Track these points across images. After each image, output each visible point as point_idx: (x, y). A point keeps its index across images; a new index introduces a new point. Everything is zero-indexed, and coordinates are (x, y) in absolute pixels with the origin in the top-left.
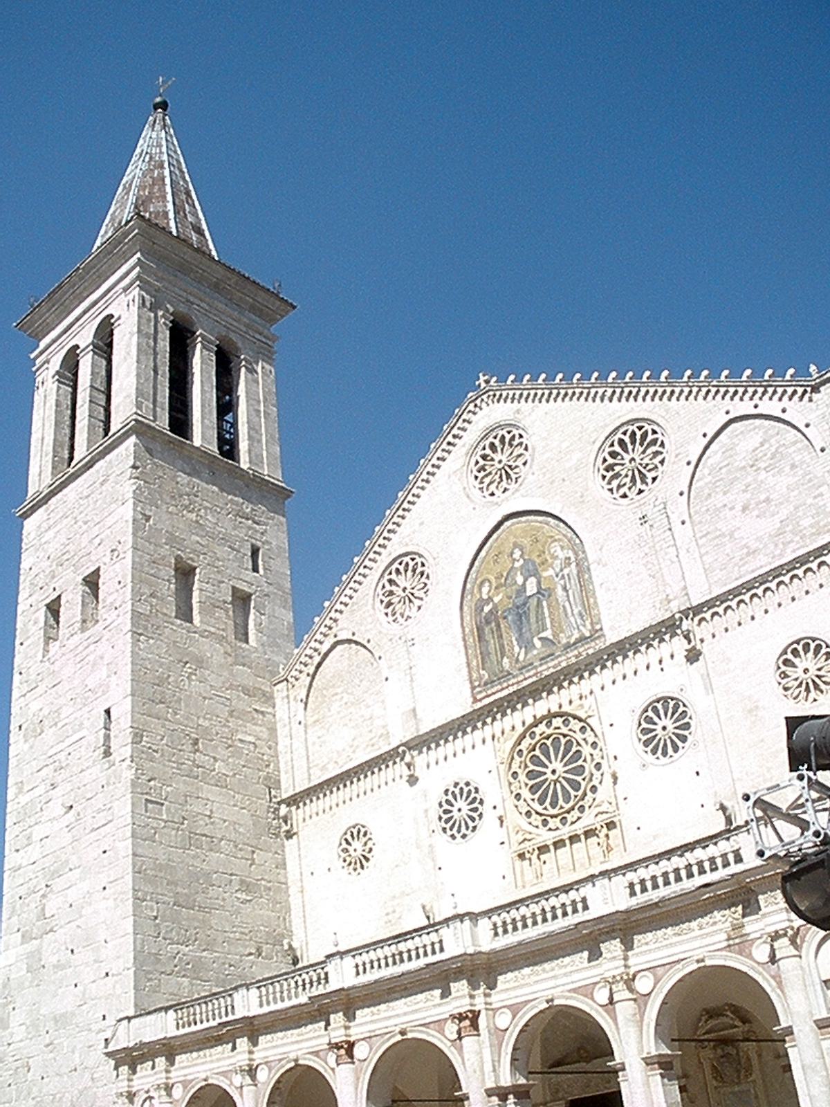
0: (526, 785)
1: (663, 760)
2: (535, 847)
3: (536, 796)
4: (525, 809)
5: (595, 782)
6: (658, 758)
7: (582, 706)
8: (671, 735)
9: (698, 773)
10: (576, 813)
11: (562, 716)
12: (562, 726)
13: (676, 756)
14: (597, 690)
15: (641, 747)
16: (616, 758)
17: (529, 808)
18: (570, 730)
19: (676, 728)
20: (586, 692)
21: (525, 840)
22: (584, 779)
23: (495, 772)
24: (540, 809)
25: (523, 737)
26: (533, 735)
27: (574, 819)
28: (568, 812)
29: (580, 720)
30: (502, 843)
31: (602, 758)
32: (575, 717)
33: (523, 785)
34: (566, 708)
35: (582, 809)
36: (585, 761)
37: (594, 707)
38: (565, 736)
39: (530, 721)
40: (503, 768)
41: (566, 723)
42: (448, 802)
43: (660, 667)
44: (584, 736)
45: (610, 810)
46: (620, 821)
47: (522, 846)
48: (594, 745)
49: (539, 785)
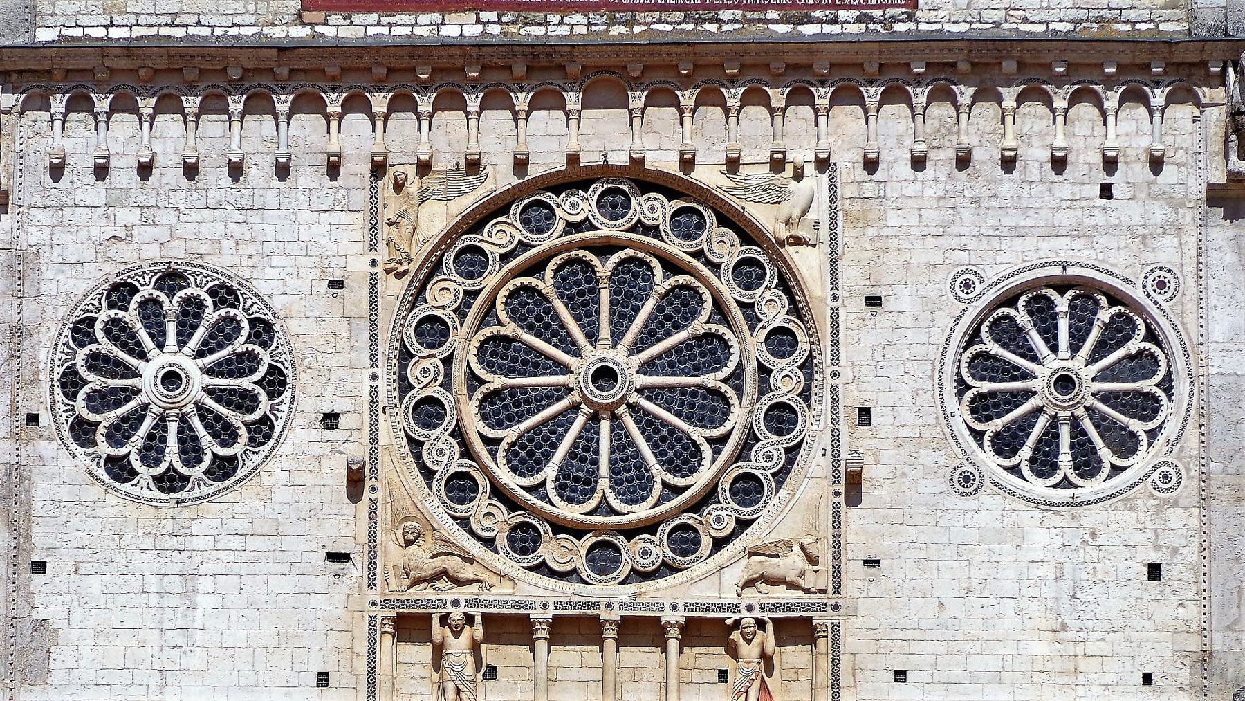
0: (474, 381)
1: (1038, 487)
2: (477, 612)
3: (510, 434)
4: (447, 461)
5: (760, 466)
6: (1015, 470)
7: (777, 197)
8: (1080, 411)
9: (1154, 571)
10: (657, 548)
11: (671, 195)
12: (666, 229)
13: (1089, 488)
14: (847, 161)
15: (961, 414)
16: (864, 415)
17: (465, 465)
18: (699, 254)
19: (1105, 397)
20: (801, 155)
21: (443, 574)
22: (718, 443)
23: (357, 295)
24: (512, 481)
25: (496, 208)
26: (541, 215)
27: (649, 564)
28: (630, 532)
29: (747, 233)
30: (344, 557)
31: (806, 395)
32: (730, 219)
33: (459, 376)
34: (708, 175)
35: (685, 541)
36: (736, 378)
37: (820, 212)
38: (672, 267)
39: (547, 162)
40: (393, 289)
41: (686, 221)
42: (117, 330)
43: (1103, 178)
44: (746, 296)
45: (810, 582)
46: (837, 627)
47: (426, 593)
48: (781, 340)
49: (523, 402)
